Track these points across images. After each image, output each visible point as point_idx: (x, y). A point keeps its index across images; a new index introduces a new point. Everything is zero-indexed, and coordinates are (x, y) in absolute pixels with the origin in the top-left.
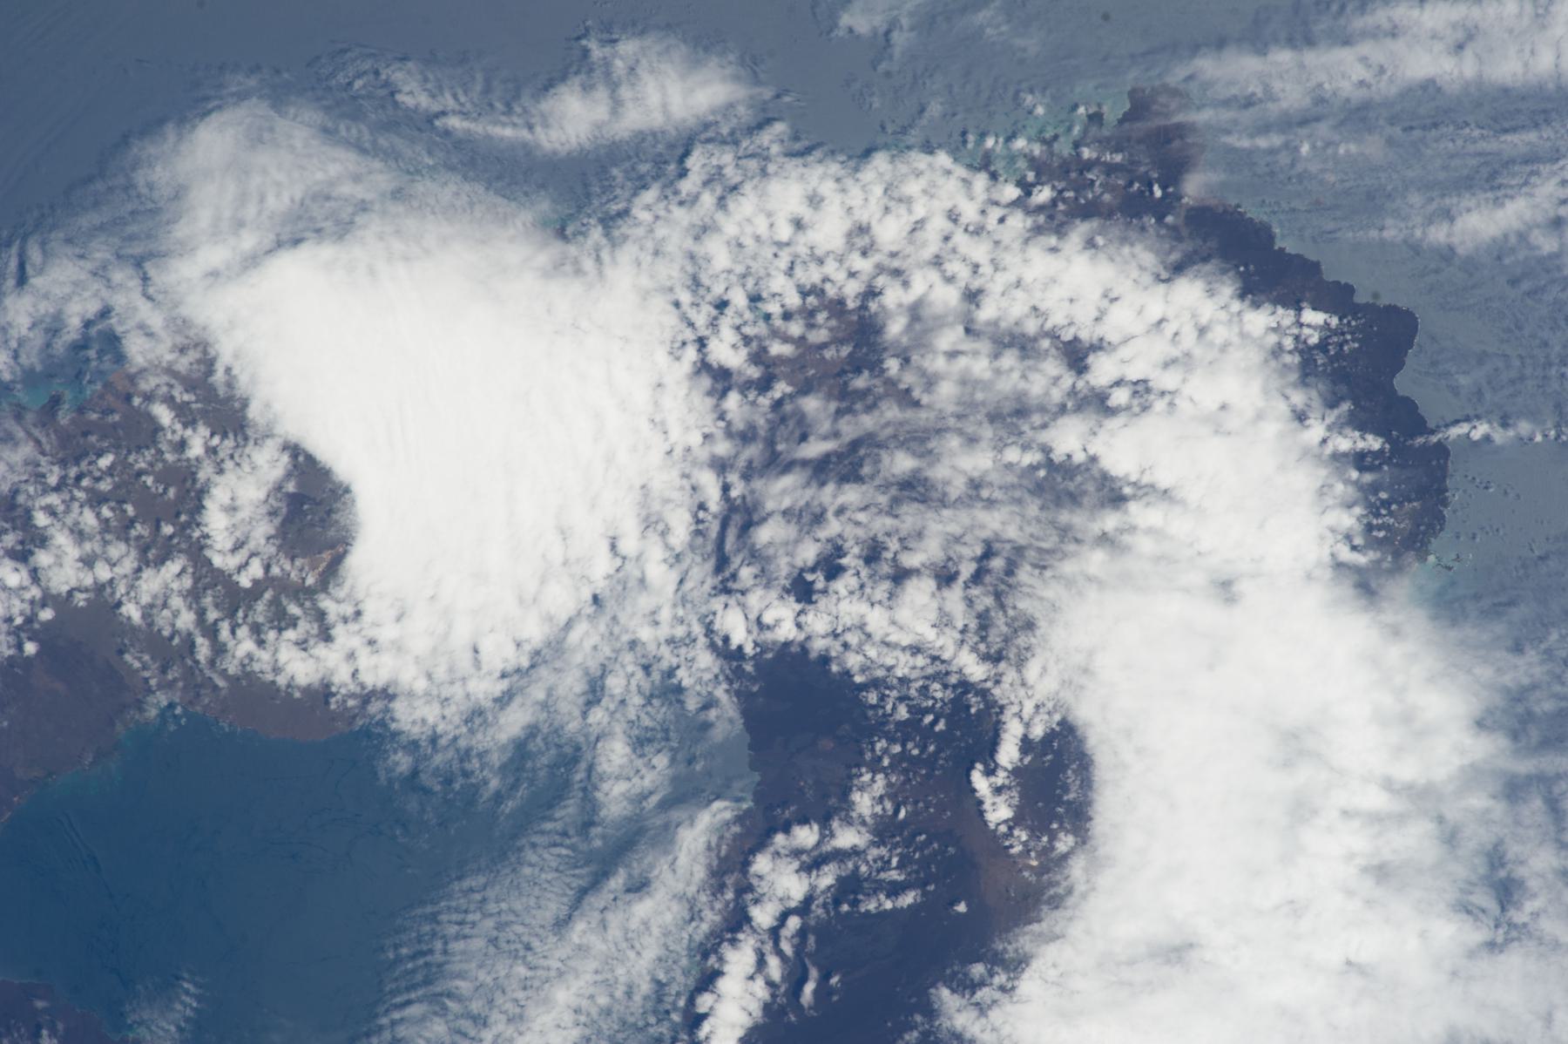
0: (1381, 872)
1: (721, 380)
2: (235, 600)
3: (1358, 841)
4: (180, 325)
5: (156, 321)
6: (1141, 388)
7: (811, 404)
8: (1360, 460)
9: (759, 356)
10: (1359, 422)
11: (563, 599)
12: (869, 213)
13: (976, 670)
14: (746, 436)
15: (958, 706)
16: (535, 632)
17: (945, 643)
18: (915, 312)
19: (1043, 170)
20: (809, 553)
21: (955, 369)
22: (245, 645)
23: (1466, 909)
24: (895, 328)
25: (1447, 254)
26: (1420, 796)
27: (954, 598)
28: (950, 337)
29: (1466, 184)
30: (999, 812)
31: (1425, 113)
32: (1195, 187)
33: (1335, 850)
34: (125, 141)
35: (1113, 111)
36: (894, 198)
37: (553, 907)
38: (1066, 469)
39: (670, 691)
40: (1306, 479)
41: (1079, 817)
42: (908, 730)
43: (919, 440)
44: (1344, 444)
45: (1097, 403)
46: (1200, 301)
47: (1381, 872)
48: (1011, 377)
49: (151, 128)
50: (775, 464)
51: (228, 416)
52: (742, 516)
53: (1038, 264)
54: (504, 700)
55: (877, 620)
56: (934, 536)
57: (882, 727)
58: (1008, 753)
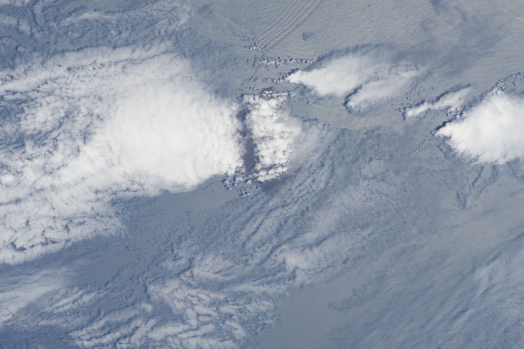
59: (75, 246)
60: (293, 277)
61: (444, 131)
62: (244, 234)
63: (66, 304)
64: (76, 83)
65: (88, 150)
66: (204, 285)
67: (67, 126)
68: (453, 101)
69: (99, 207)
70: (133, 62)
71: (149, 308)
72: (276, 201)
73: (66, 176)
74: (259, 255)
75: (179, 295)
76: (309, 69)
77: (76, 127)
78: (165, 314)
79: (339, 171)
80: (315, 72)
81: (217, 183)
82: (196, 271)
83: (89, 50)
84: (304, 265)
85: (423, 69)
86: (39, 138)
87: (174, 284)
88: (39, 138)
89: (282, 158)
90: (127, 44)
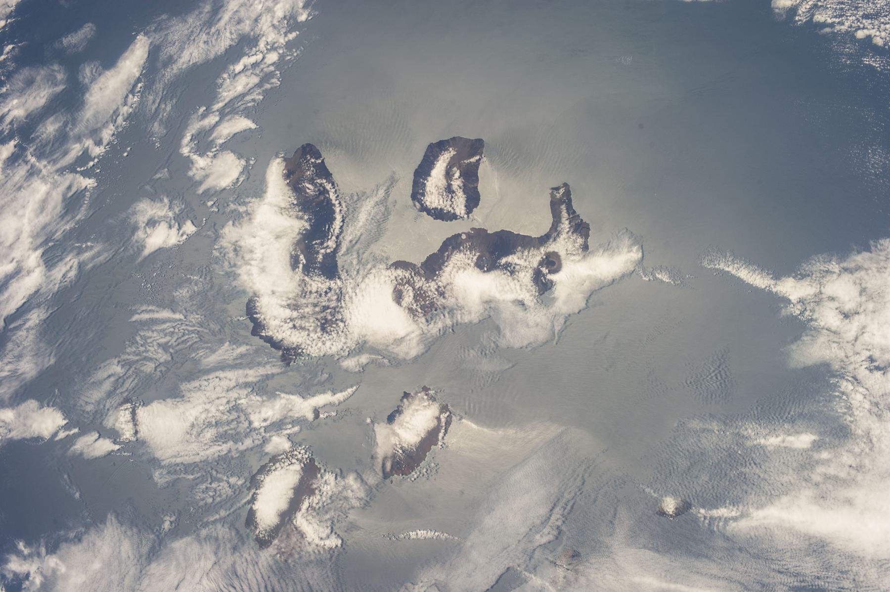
0: (251, 252)
1: (342, 321)
2: (408, 282)
3: (255, 256)
4: (418, 324)
5: (421, 325)
6: (286, 322)
7: (330, 317)
8: (257, 313)
9: (337, 324)
10: (257, 319)
11: (363, 285)
12: (323, 347)
13: (306, 278)
14: (338, 312)
15: (308, 273)
16: (367, 280)
17: (311, 282)
18: (316, 332)
19: (300, 355)
20: (329, 295)
21: (310, 324)
22: (407, 275)
23: (240, 247)
24: (319, 330)
25: (247, 344)
26: (247, 263)
27: (309, 289)
28: (311, 329)
29: (245, 355)
30: (302, 257)
31: (251, 365)
32: (280, 353)
33: (257, 255)
34: (426, 352)
35: (292, 363)
36: (320, 349)
37: (362, 237)
38: (295, 309)
39: (347, 272)
40: (263, 310)
41: (291, 257)
42: (315, 269)
43: (314, 314)
44: (258, 316)
45: (292, 320)
46: (278, 336)
47: (251, 252)
48: (304, 323)
49: (423, 354)
50: (334, 308)
51: (411, 310)
52: (339, 300)
53: (300, 340)
54: (371, 269)
55: (320, 285)
56: (312, 299)
57: (319, 268)
58: (301, 266)
59: (198, 377)
60: (119, 362)
61: (65, 422)
62: (136, 381)
63: (201, 353)
64: (196, 448)
65: (192, 419)
66: (151, 359)
67: (200, 430)
68: (62, 435)
69: (188, 394)
70: (175, 457)
71: (171, 350)
72: (125, 395)
73: (200, 408)
74: (130, 372)
75: (160, 355)
76: (113, 451)
77: (195, 430)
78: (165, 347)
79: (102, 407)
80: (110, 449)
81: (145, 404)
82: (153, 366)
83: (191, 462)
84: (114, 367)
85: (72, 449)
86: (210, 425)
87: (162, 360)
88: (210, 425)
89: (122, 413)
90: (178, 465)
